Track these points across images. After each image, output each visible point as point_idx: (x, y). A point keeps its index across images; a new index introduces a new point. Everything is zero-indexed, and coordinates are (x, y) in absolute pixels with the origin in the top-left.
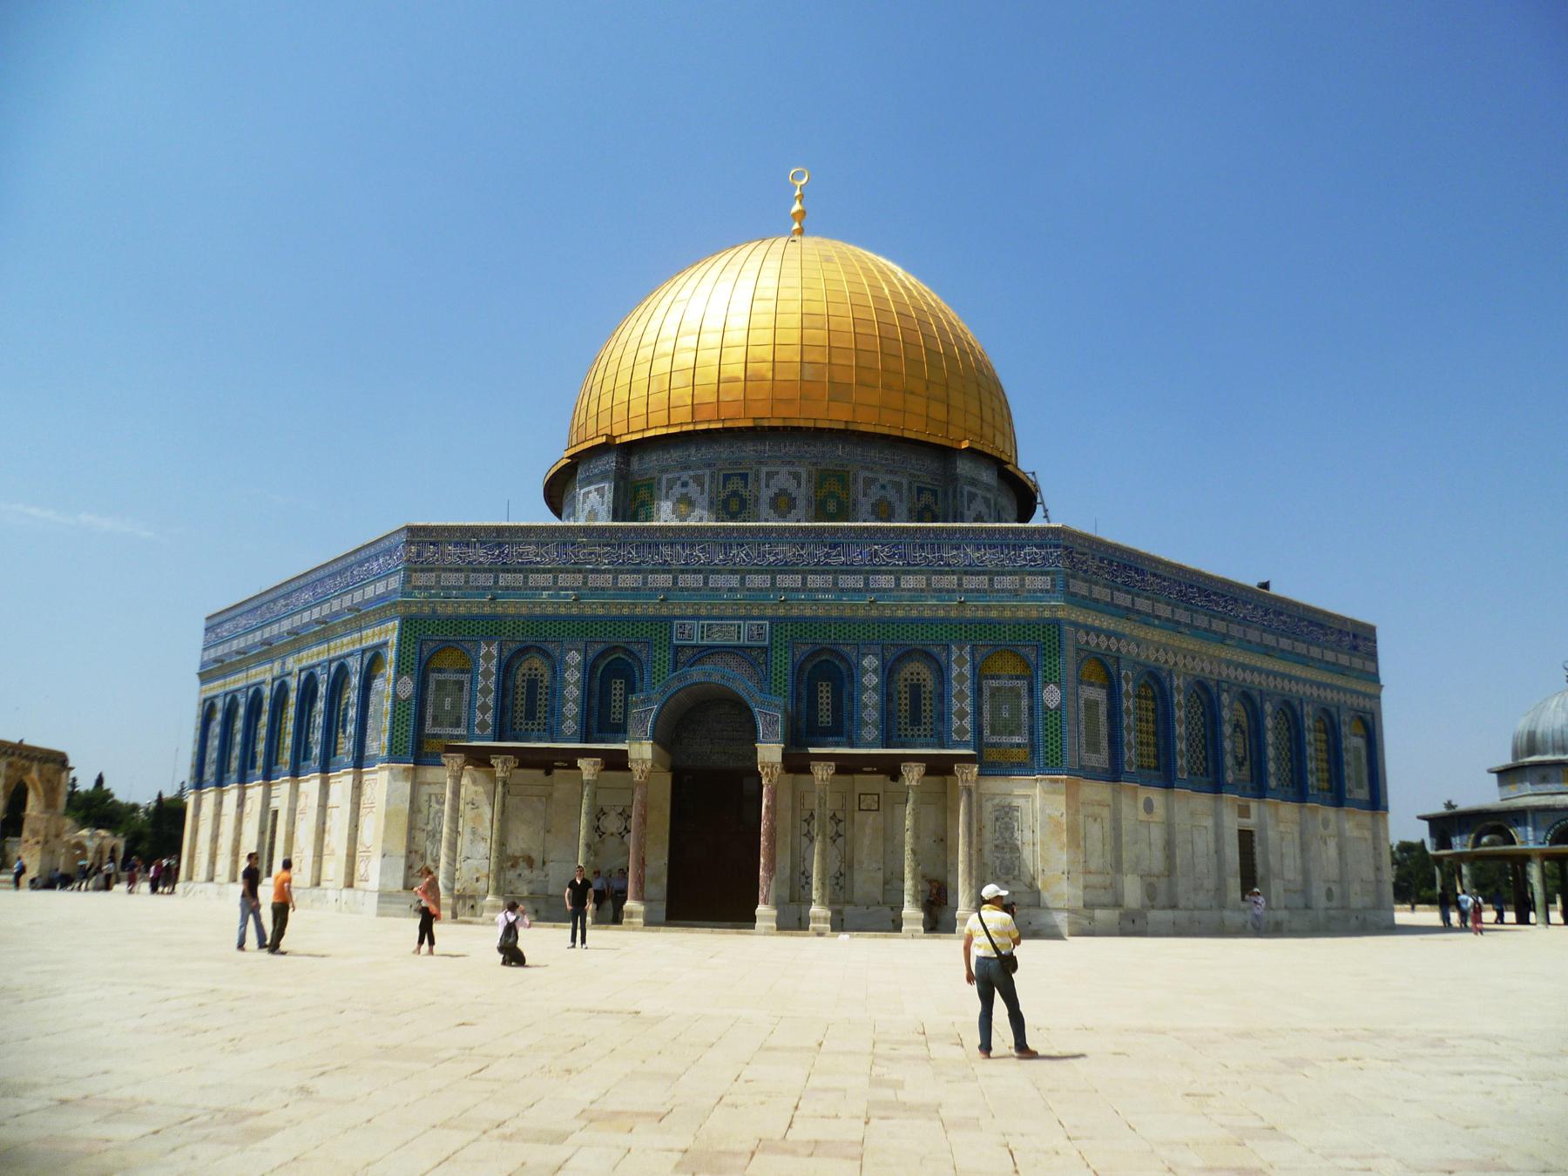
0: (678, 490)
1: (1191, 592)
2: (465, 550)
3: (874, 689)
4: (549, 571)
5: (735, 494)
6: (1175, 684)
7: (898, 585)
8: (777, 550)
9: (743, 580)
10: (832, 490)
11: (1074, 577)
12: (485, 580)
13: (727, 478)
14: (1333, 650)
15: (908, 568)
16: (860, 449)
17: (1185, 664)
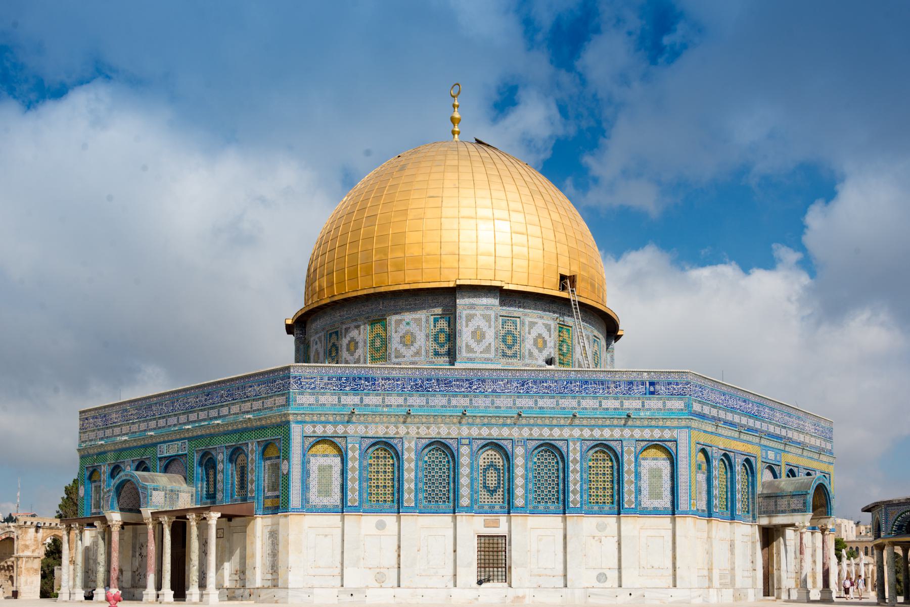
0: (315, 347)
1: (427, 384)
2: (96, 420)
3: (223, 471)
4: (119, 426)
5: (334, 345)
6: (406, 445)
7: (229, 412)
8: (189, 401)
9: (178, 419)
10: (378, 332)
11: (302, 394)
12: (101, 434)
13: (331, 334)
14: (616, 398)
15: (234, 402)
16: (392, 302)
17: (418, 433)
